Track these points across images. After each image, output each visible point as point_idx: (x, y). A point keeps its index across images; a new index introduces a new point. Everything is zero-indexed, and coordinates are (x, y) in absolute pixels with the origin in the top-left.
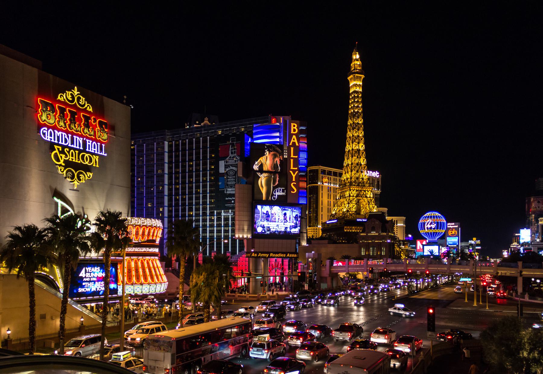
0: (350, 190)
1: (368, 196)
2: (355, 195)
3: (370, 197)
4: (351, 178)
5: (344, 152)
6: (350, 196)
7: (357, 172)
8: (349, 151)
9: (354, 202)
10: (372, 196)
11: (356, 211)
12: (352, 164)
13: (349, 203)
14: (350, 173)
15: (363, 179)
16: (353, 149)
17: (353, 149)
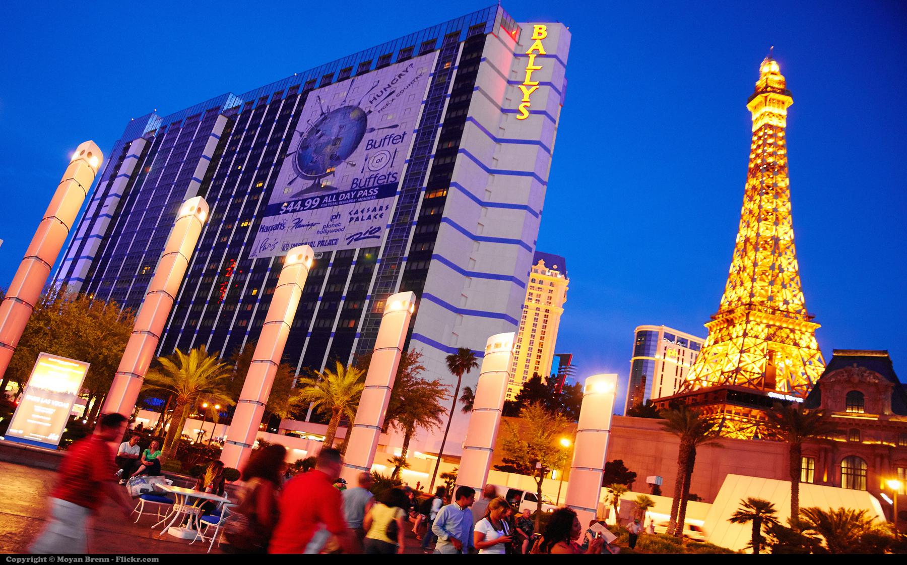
0: (748, 322)
1: (803, 343)
2: (763, 336)
3: (808, 347)
4: (752, 295)
5: (736, 245)
6: (745, 335)
7: (772, 283)
8: (747, 240)
9: (759, 352)
10: (814, 344)
11: (764, 375)
12: (755, 264)
13: (742, 352)
14: (748, 284)
15: (786, 302)
16: (758, 235)
17: (758, 235)
